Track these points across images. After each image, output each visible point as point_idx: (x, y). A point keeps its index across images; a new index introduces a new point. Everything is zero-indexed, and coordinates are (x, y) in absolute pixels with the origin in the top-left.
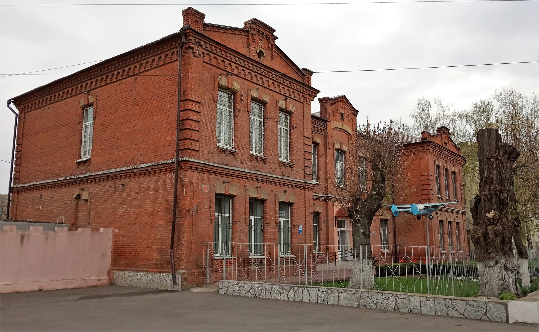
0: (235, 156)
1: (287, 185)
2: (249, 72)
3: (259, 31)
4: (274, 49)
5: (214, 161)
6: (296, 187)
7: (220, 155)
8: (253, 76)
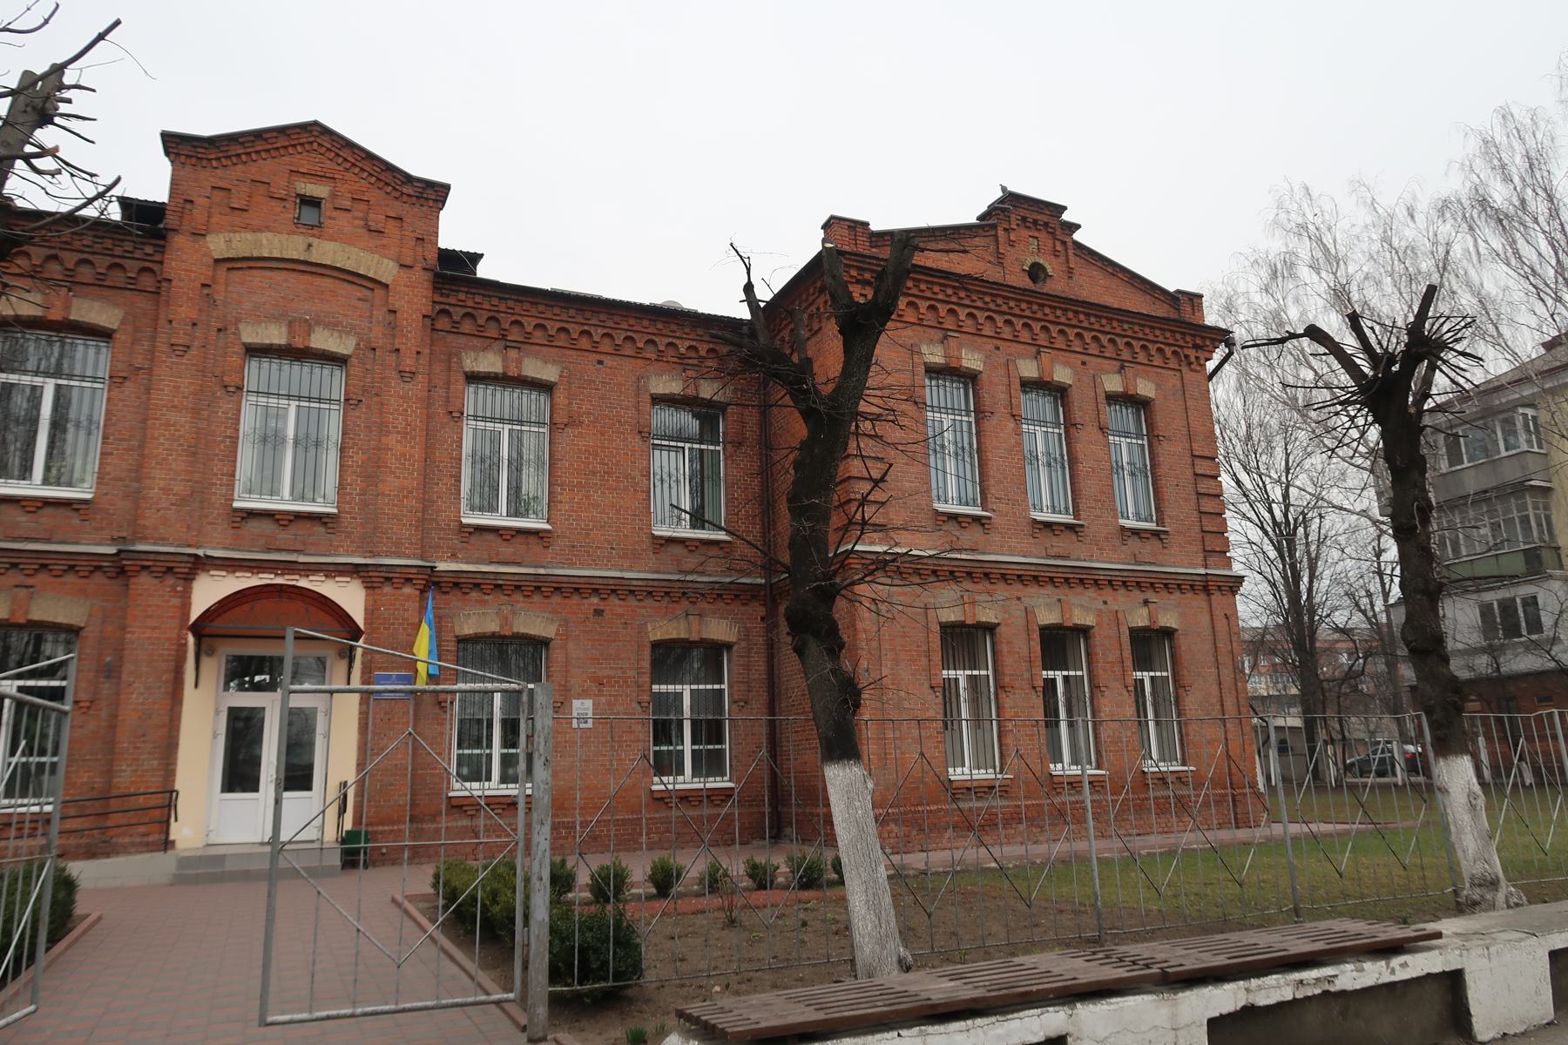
0: (987, 526)
1: (999, 576)
2: (1042, 327)
3: (1024, 219)
4: (1071, 252)
5: (923, 547)
6: (1192, 586)
7: (1130, 542)
8: (1019, 327)
